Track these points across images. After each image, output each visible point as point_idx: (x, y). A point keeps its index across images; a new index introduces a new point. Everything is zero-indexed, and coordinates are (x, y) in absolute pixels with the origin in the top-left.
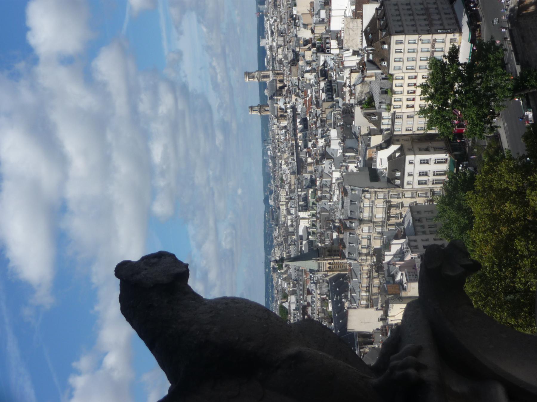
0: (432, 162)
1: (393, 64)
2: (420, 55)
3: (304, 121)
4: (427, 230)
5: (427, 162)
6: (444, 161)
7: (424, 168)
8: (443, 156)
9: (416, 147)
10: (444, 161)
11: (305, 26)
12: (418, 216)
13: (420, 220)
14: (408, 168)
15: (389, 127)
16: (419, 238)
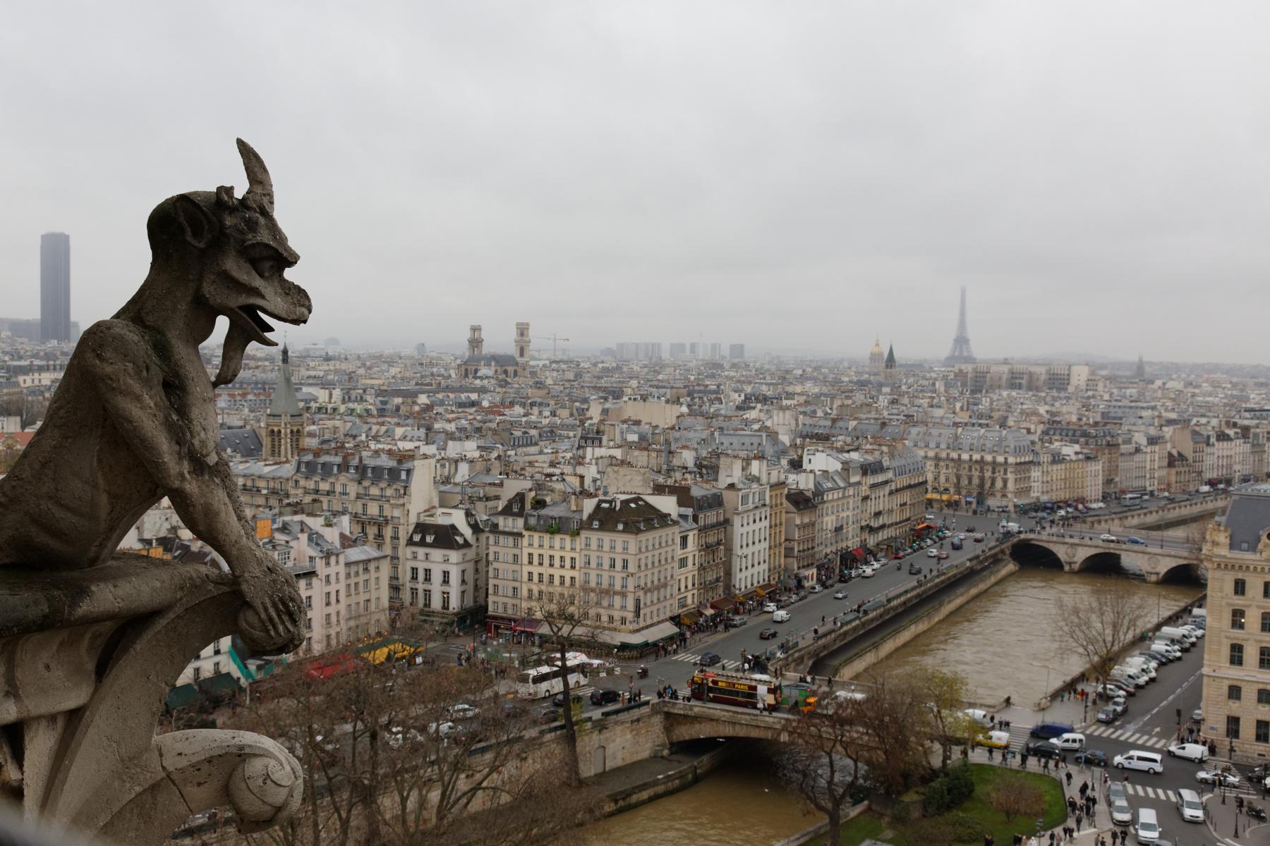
0: (446, 589)
1: (594, 537)
2: (606, 575)
3: (473, 404)
4: (352, 581)
5: (446, 581)
6: (445, 606)
7: (437, 577)
8: (454, 604)
9: (470, 567)
10: (445, 606)
11: (605, 412)
12: (372, 566)
13: (366, 570)
14: (437, 554)
15: (501, 528)
16: (341, 569)
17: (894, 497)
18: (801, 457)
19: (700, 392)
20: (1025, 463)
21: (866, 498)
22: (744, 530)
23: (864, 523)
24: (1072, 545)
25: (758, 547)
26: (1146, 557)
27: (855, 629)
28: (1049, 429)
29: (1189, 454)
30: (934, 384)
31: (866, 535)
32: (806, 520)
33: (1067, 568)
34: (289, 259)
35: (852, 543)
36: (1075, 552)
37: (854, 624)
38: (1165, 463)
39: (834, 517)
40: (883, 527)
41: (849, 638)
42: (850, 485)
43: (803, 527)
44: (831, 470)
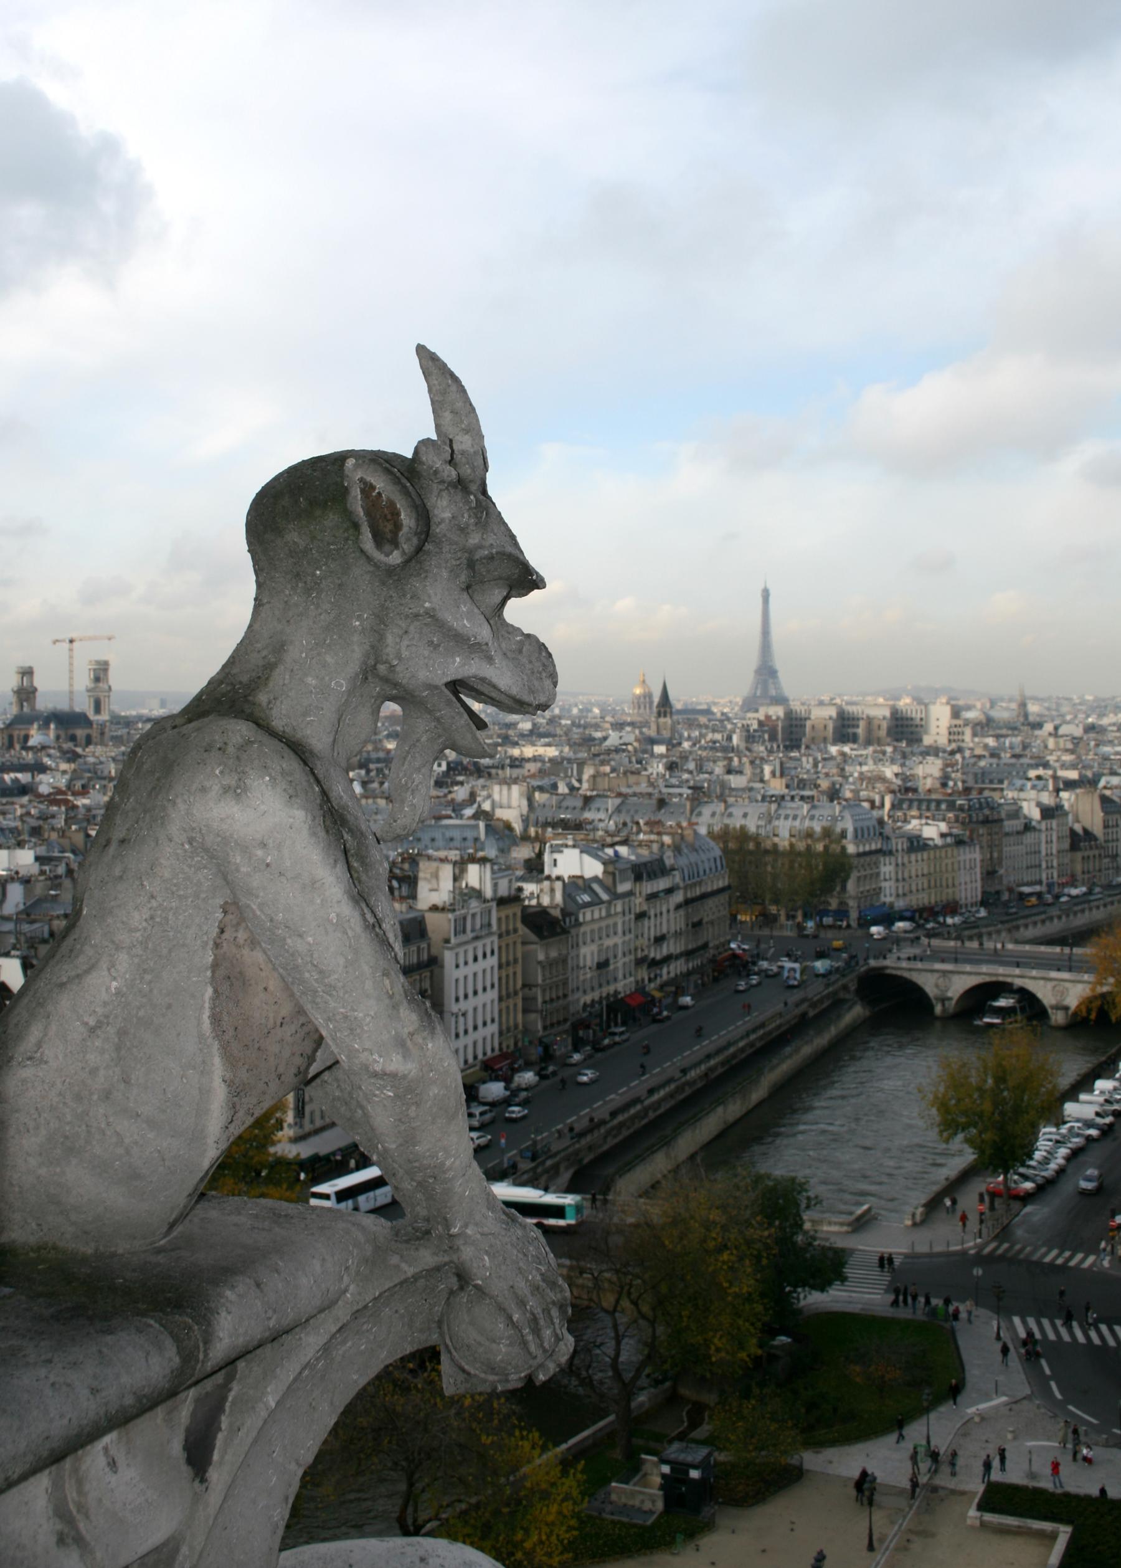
17: (682, 912)
18: (540, 855)
19: (378, 760)
20: (871, 853)
21: (641, 916)
22: (460, 973)
23: (639, 955)
24: (945, 973)
25: (482, 998)
26: (1050, 985)
27: (633, 1118)
28: (901, 801)
29: (1098, 830)
30: (730, 738)
31: (643, 973)
32: (554, 954)
33: (938, 1009)
34: (525, 580)
35: (623, 985)
36: (947, 982)
37: (632, 1111)
38: (1066, 845)
39: (594, 948)
40: (668, 959)
41: (625, 1133)
42: (616, 896)
43: (549, 965)
44: (588, 875)
